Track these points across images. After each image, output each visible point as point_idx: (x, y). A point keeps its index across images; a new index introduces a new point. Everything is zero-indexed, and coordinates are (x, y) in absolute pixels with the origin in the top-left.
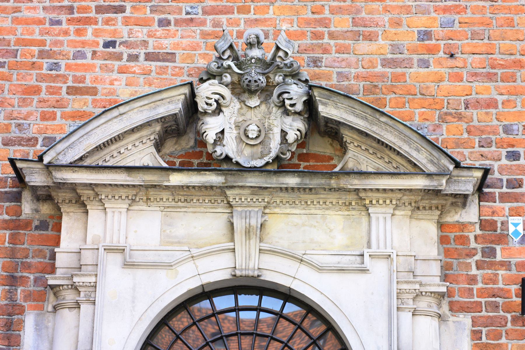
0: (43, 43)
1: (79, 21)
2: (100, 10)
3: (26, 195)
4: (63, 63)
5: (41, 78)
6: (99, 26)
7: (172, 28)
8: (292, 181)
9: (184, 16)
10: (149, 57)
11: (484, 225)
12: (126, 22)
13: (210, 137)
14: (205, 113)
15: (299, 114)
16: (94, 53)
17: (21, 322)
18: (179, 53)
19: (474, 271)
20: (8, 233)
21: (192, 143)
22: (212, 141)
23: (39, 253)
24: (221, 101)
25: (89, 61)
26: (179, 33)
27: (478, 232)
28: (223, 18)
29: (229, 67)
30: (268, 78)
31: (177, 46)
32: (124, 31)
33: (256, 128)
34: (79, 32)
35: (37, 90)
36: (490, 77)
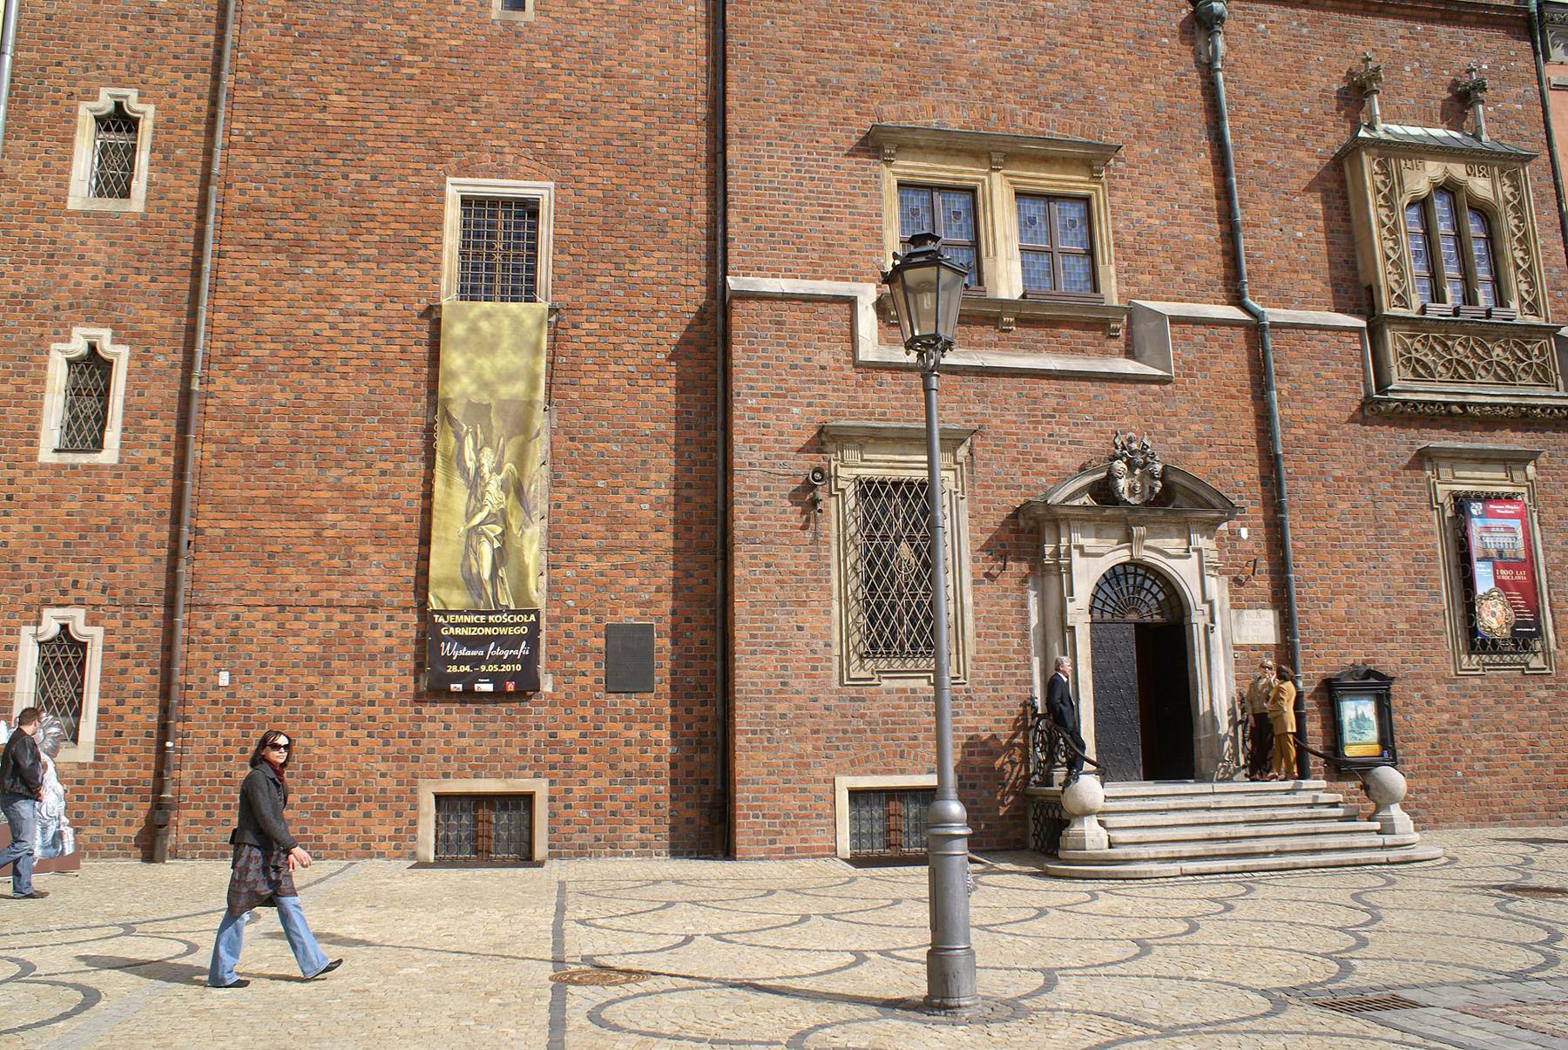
12: (1057, 423)
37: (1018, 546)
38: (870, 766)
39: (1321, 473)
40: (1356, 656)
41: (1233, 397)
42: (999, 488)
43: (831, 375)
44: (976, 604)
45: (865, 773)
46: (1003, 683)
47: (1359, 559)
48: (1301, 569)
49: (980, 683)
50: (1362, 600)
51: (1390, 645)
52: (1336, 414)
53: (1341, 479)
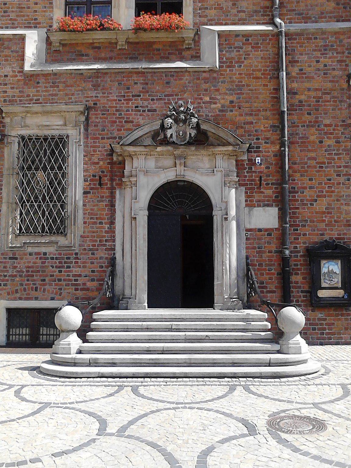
0: (116, 107)
1: (126, 100)
2: (133, 96)
3: (114, 154)
4: (123, 113)
5: (117, 118)
6: (133, 101)
7: (155, 101)
9: (159, 97)
10: (149, 111)
11: (249, 160)
12: (141, 99)
13: (169, 136)
15: (195, 128)
16: (132, 110)
18: (158, 109)
19: (246, 174)
20: (110, 166)
23: (119, 172)
25: (130, 112)
27: (247, 162)
28: (171, 98)
31: (157, 107)
34: (127, 104)
35: (115, 122)
36: (251, 115)
38: (18, 295)
39: (317, 122)
41: (257, 78)
43: (9, 80)
44: (84, 205)
45: (15, 299)
46: (97, 250)
47: (338, 175)
49: (85, 249)
50: (338, 200)
53: (330, 125)
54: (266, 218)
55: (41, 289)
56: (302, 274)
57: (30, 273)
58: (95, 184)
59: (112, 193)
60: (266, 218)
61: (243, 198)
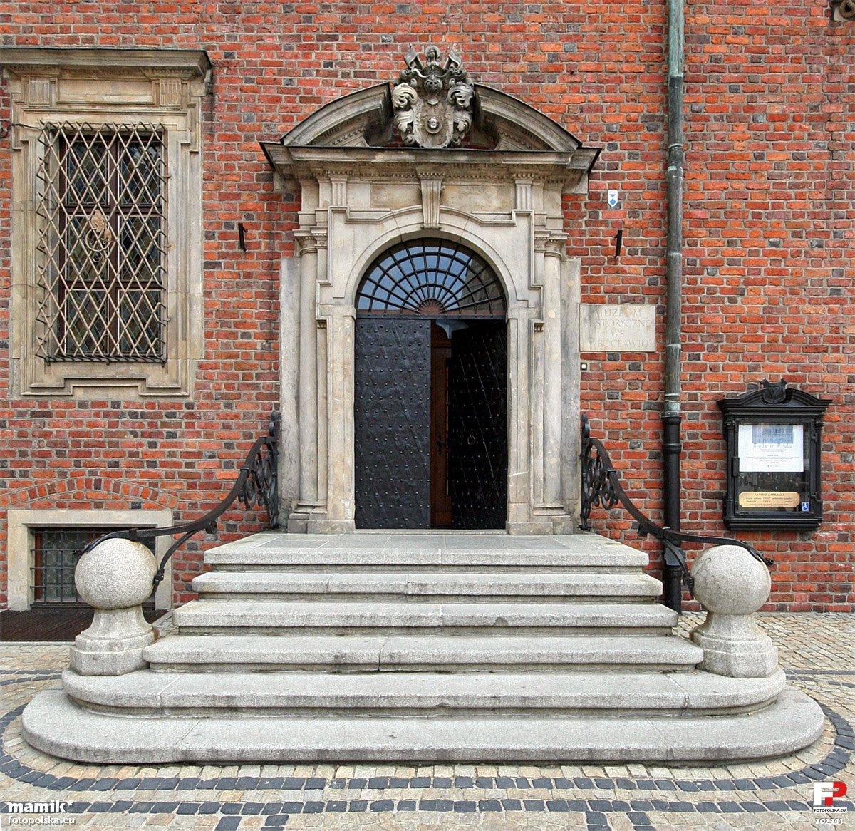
0: (279, 64)
1: (305, 47)
2: (320, 38)
3: (276, 176)
4: (295, 79)
5: (281, 91)
6: (320, 51)
7: (373, 52)
8: (462, 159)
9: (381, 43)
10: (357, 74)
11: (591, 196)
12: (340, 48)
13: (404, 126)
14: (399, 109)
16: (318, 71)
17: (279, 265)
19: (584, 228)
21: (390, 138)
22: (405, 130)
23: (288, 217)
24: (411, 99)
25: (314, 77)
26: (378, 56)
27: (587, 200)
29: (416, 74)
30: (444, 82)
31: (376, 66)
32: (338, 54)
33: (435, 120)
35: (278, 100)
36: (598, 90)
37: (270, 217)
38: (56, 498)
39: (750, 109)
40: (774, 371)
42: (248, 139)
44: (207, 294)
45: (48, 506)
46: (238, 397)
47: (795, 235)
48: (699, 245)
49: (209, 396)
50: (793, 292)
51: (832, 356)
52: (786, 20)
53: (782, 118)
54: (629, 328)
55: (108, 483)
56: (708, 456)
57: (82, 448)
58: (231, 246)
59: (270, 266)
60: (629, 328)
61: (576, 283)
